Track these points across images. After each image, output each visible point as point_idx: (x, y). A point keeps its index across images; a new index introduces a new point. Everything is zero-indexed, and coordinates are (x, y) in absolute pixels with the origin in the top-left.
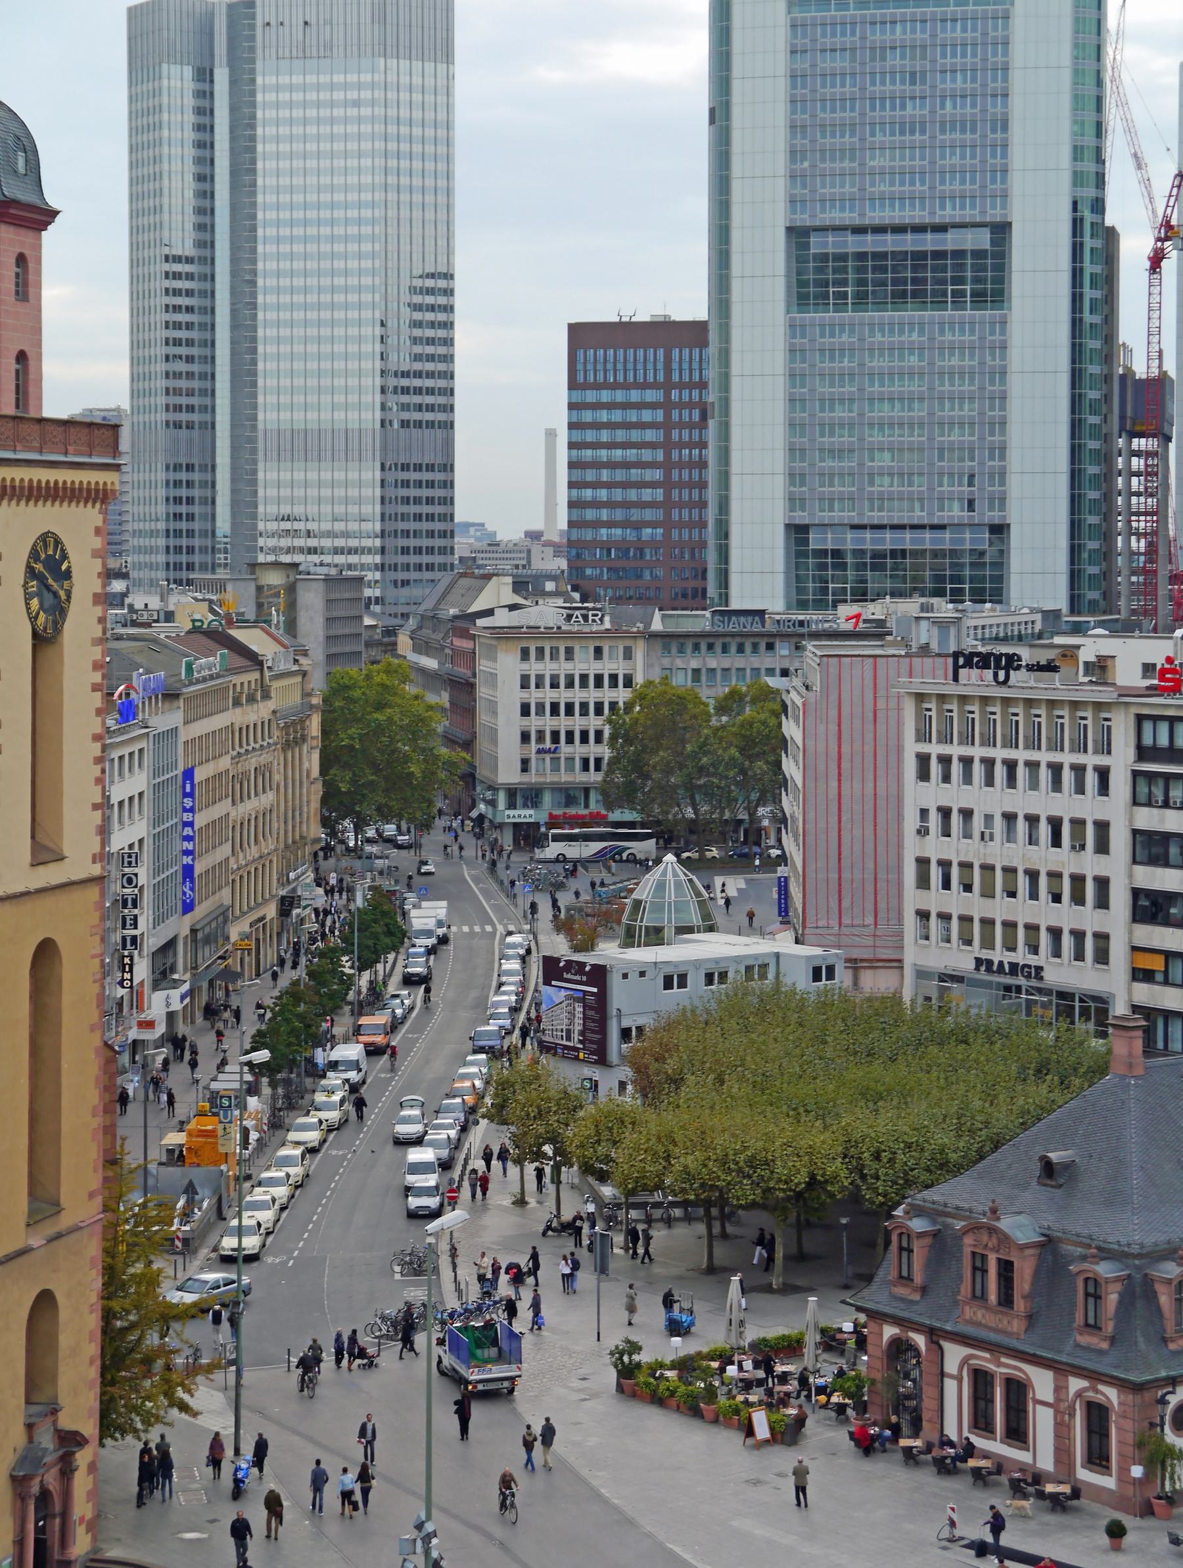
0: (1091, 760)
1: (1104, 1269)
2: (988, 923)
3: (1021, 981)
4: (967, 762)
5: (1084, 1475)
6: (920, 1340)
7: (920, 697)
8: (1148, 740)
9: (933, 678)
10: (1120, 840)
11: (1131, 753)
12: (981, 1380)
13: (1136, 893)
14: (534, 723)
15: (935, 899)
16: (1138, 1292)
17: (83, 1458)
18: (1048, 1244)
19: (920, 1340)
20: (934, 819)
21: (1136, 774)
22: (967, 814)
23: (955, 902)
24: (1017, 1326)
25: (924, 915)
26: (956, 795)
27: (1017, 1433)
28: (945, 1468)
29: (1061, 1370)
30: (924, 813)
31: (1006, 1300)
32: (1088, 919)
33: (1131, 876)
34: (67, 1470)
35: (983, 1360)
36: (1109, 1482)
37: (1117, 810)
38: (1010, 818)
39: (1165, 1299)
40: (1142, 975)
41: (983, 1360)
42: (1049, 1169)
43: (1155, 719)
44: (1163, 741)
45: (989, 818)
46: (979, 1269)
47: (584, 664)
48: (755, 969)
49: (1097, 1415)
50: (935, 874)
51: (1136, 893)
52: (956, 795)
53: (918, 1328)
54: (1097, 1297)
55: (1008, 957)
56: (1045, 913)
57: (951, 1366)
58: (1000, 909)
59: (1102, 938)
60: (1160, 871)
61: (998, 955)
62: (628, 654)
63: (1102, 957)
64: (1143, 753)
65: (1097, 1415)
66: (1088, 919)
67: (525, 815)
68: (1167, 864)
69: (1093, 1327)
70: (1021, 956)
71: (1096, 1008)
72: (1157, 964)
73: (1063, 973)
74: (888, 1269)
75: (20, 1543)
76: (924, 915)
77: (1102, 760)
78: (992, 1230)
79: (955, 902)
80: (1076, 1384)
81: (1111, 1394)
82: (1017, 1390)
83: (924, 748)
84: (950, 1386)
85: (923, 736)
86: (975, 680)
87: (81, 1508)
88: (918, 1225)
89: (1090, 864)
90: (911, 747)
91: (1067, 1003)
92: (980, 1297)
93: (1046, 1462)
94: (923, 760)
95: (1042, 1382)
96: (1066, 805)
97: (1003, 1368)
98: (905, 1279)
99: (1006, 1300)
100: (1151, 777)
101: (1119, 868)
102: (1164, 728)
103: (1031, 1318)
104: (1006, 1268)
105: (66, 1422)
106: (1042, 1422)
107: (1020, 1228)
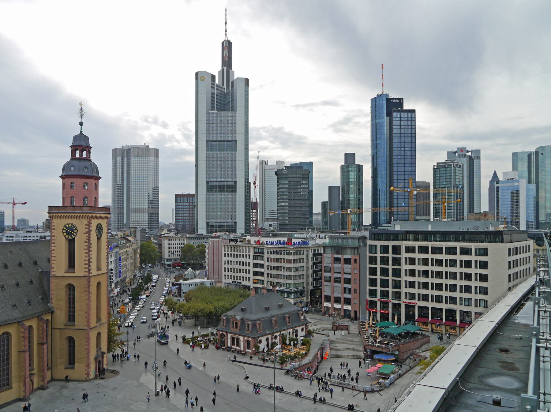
0: (248, 254)
1: (250, 323)
2: (234, 276)
4: (231, 254)
5: (247, 350)
6: (225, 333)
7: (225, 246)
9: (226, 243)
10: (252, 264)
12: (233, 339)
14: (170, 250)
15: (227, 273)
16: (254, 325)
17: (105, 355)
18: (242, 320)
19: (225, 333)
22: (231, 261)
23: (229, 273)
24: (238, 331)
25: (225, 275)
26: (229, 259)
27: (238, 345)
28: (228, 350)
29: (244, 336)
31: (236, 327)
32: (247, 275)
34: (103, 357)
35: (233, 336)
36: (250, 351)
37: (251, 260)
38: (237, 262)
39: (258, 326)
40: (254, 283)
41: (233, 336)
42: (242, 309)
46: (233, 323)
47: (178, 241)
48: (202, 283)
49: (249, 342)
50: (227, 270)
52: (229, 259)
56: (242, 275)
57: (229, 337)
59: (249, 278)
61: (235, 281)
63: (249, 280)
64: (255, 253)
65: (249, 342)
66: (247, 275)
67: (169, 263)
69: (248, 330)
70: (238, 281)
71: (248, 287)
72: (257, 281)
73: (244, 283)
74: (220, 324)
75: (96, 368)
76: (225, 275)
79: (229, 273)
80: (246, 338)
81: (251, 339)
82: (238, 340)
84: (229, 339)
85: (225, 251)
86: (232, 243)
87: (105, 362)
88: (224, 318)
89: (248, 268)
90: (223, 252)
92: (233, 327)
94: (225, 254)
95: (241, 338)
96: (244, 260)
97: (236, 336)
98: (223, 325)
99: (236, 327)
101: (251, 268)
103: (240, 330)
104: (236, 323)
105: (103, 350)
106: (241, 344)
107: (238, 317)
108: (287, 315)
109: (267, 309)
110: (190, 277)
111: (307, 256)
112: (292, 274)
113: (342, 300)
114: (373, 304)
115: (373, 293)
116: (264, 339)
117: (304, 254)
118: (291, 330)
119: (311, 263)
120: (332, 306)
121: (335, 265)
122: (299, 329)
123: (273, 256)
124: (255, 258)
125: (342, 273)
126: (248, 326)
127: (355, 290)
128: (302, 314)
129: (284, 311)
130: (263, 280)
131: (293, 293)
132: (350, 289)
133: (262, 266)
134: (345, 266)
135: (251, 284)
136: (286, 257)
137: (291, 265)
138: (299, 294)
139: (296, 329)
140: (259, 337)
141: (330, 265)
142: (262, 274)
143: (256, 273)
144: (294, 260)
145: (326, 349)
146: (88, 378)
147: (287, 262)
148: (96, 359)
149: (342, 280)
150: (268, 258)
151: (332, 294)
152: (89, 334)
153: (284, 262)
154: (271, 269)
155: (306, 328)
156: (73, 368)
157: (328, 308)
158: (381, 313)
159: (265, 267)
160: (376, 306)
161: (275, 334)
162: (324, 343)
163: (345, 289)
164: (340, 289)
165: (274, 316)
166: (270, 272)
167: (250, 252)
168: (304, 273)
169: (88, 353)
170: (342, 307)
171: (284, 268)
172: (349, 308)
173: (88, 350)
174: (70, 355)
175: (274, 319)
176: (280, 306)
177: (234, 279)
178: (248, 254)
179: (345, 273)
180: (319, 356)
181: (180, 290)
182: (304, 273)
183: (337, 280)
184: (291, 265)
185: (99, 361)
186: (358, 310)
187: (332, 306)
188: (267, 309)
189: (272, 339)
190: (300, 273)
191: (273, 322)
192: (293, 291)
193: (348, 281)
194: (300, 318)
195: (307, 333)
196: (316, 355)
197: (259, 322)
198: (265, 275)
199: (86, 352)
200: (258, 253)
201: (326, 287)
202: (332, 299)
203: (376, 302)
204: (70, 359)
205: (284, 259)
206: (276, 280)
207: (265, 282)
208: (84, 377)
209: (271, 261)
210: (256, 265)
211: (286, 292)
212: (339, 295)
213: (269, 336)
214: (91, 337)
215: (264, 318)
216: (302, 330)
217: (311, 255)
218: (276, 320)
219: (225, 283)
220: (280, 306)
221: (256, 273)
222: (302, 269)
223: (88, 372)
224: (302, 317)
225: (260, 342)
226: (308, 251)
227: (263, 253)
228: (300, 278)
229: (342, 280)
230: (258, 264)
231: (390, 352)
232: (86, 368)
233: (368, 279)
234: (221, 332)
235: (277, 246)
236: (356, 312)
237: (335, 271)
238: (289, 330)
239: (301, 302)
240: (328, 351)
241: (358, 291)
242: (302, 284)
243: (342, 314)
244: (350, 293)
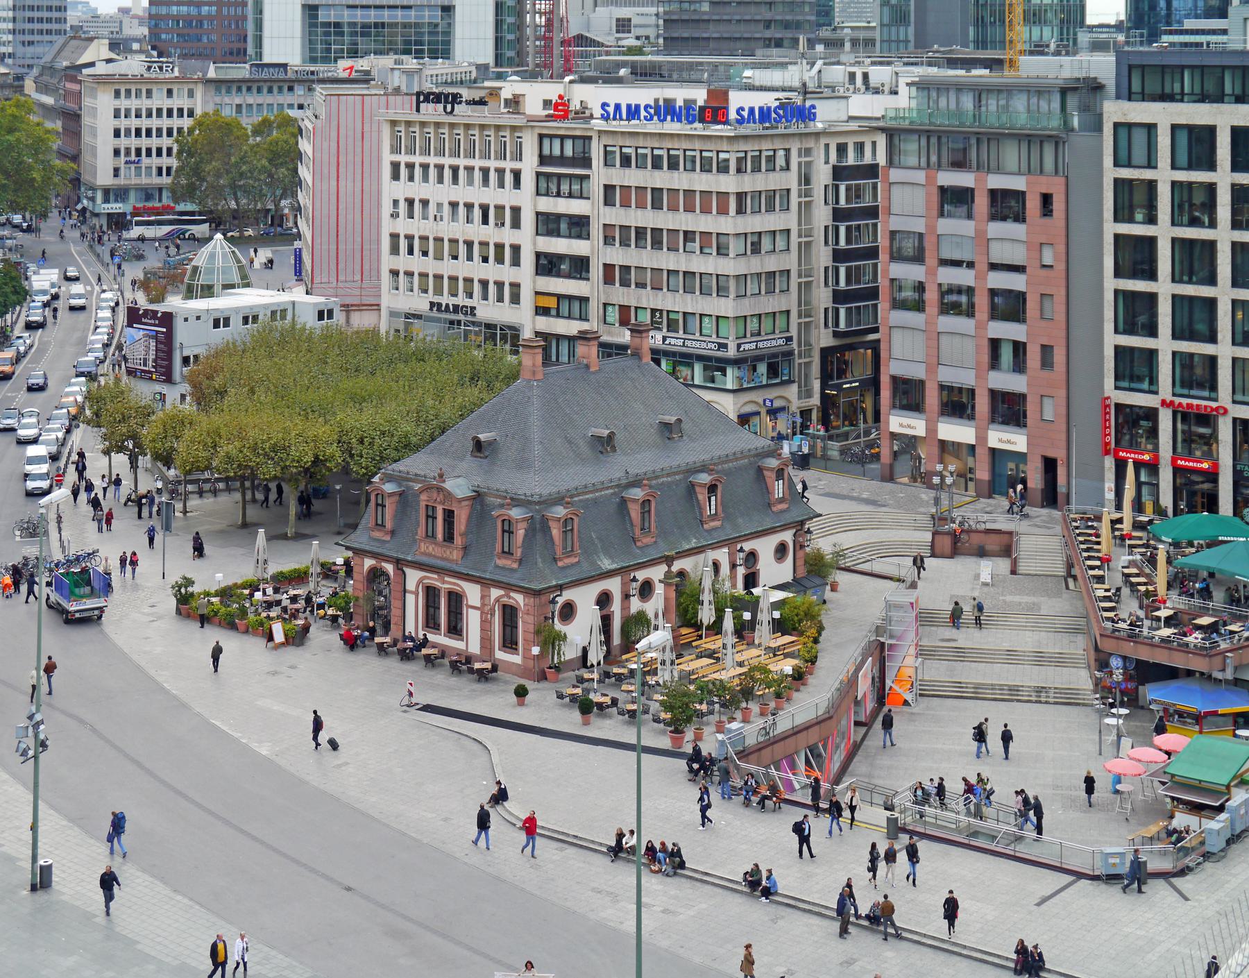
0: (508, 165)
1: (516, 513)
2: (438, 278)
3: (461, 317)
4: (425, 167)
6: (389, 568)
8: (546, 152)
10: (528, 219)
11: (536, 160)
12: (431, 594)
13: (538, 255)
15: (403, 262)
18: (478, 497)
19: (389, 568)
20: (403, 206)
21: (538, 174)
22: (425, 203)
23: (417, 263)
24: (456, 555)
25: (395, 273)
26: (418, 190)
29: (485, 583)
30: (396, 202)
31: (449, 537)
32: (506, 273)
33: (535, 244)
35: (433, 579)
36: (516, 659)
37: (527, 200)
38: (454, 205)
39: (556, 532)
40: (542, 311)
43: (551, 137)
44: (557, 152)
45: (440, 205)
46: (431, 517)
47: (159, 100)
48: (278, 313)
49: (510, 613)
50: (403, 244)
51: (538, 255)
52: (418, 190)
53: (388, 559)
54: (510, 533)
55: (453, 301)
56: (477, 270)
57: (411, 584)
58: (447, 267)
59: (515, 286)
60: (554, 240)
61: (446, 299)
62: (191, 94)
63: (515, 299)
64: (543, 160)
65: (510, 613)
66: (506, 273)
68: (559, 235)
70: (461, 300)
71: (510, 335)
72: (552, 303)
73: (490, 311)
74: (368, 519)
76: (395, 273)
79: (417, 263)
80: (495, 593)
81: (519, 599)
82: (456, 600)
84: (410, 599)
88: (389, 488)
89: (507, 236)
91: (491, 331)
92: (431, 536)
93: (474, 647)
95: (472, 593)
96: (492, 196)
97: (446, 584)
99: (449, 537)
100: (548, 176)
101: (528, 239)
102: (557, 143)
104: (449, 515)
106: (472, 621)
107: (459, 487)
108: (705, 478)
109: (605, 444)
110: (217, 280)
111: (806, 179)
112: (729, 266)
113: (982, 404)
114: (1133, 424)
115: (1136, 368)
117: (788, 168)
118: (722, 555)
119: (822, 215)
120: (932, 430)
121: (945, 226)
122: (765, 547)
123: (633, 177)
124: (546, 184)
125: (982, 265)
126: (508, 530)
127: (1046, 350)
128: (780, 474)
129: (688, 453)
130: (584, 300)
131: (736, 362)
132: (1019, 348)
133: (579, 226)
134: (996, 229)
136: (702, 182)
137: (727, 224)
138: (762, 368)
139: (748, 546)
140: (561, 588)
141: (919, 226)
142: (580, 266)
143: (548, 265)
144: (741, 196)
145: (899, 654)
147: (706, 210)
149: (982, 302)
150: (609, 189)
151: (932, 369)
153: (689, 209)
154: (625, 243)
155: (799, 546)
157: (910, 443)
158: (1177, 470)
159: (596, 230)
160: (1153, 433)
161: (641, 575)
162: (887, 619)
163: (995, 344)
164: (969, 346)
165: (636, 483)
166: (618, 256)
168: (791, 261)
170: (982, 438)
171: (689, 236)
172: (1017, 441)
175: (638, 493)
177: (439, 291)
179: (994, 267)
180: (864, 686)
181: (166, 344)
183: (956, 302)
184: (727, 224)
186: (1059, 453)
187: (932, 430)
188: (605, 444)
189: (626, 597)
190: (771, 264)
191: (635, 511)
192: (732, 352)
193: (1010, 306)
194: (768, 491)
195: (802, 572)
196: (852, 682)
197: (560, 511)
198: (596, 271)
200: (562, 160)
201: (897, 336)
202: (932, 398)
203: (1151, 414)
205: (689, 193)
207: (594, 309)
209: (626, 204)
210: (549, 224)
211: (700, 358)
212: (965, 378)
213: (614, 585)
215: (585, 489)
216: (781, 550)
217: (822, 175)
218: (646, 503)
219: (393, 314)
221: (548, 265)
222: (781, 244)
224: (779, 489)
225: (568, 611)
226: (808, 152)
227: (586, 162)
228: (770, 291)
229: (982, 302)
230: (558, 217)
231: (1229, 675)
233: (1109, 297)
234: (369, 563)
235: (654, 127)
236: (1050, 465)
237: (947, 254)
238: (712, 555)
239: (773, 412)
240: (910, 661)
241: (1059, 356)
242: (781, 322)
243: (983, 474)
244: (1019, 366)
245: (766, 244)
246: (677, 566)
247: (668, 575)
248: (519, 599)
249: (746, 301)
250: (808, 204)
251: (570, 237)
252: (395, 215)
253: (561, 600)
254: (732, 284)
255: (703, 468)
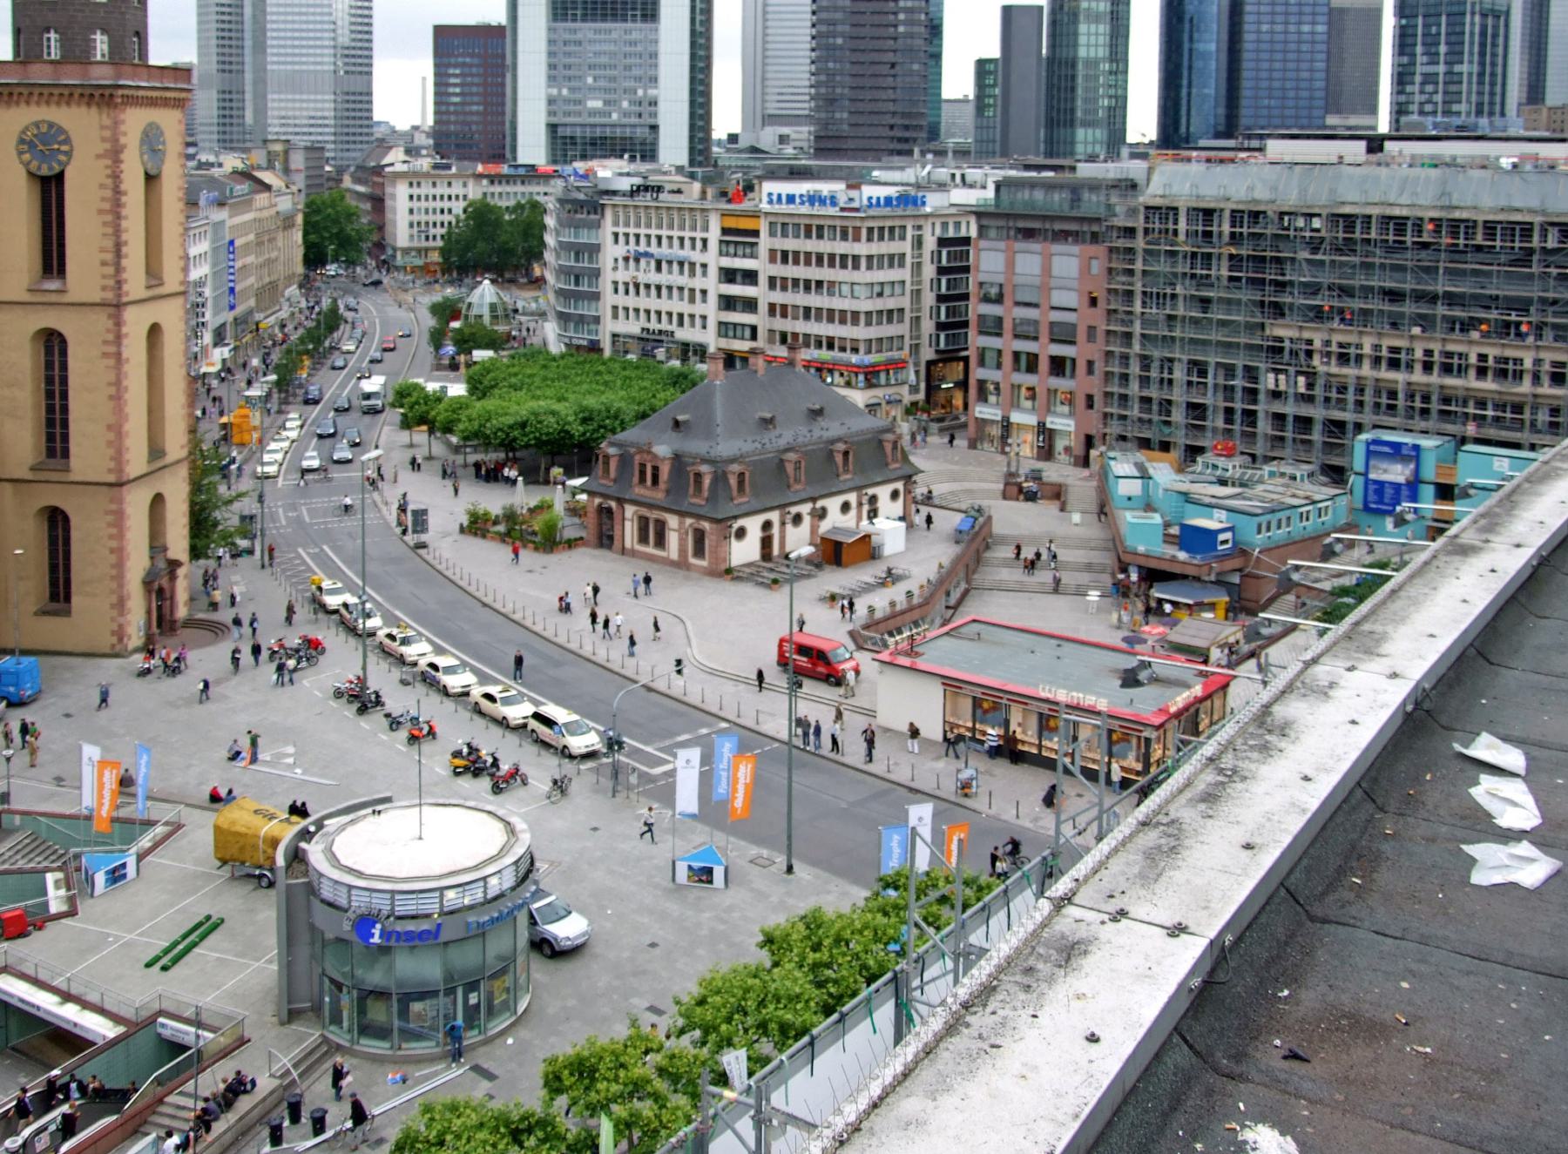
1: (704, 468)
5: (693, 561)
6: (613, 504)
12: (643, 523)
16: (720, 478)
17: (181, 572)
19: (613, 504)
23: (631, 301)
29: (682, 514)
34: (173, 577)
35: (645, 512)
36: (704, 563)
37: (713, 259)
49: (700, 537)
50: (621, 288)
51: (721, 296)
59: (704, 318)
75: (149, 612)
77: (704, 235)
78: (649, 452)
80: (689, 521)
81: (706, 525)
82: (661, 527)
83: (616, 229)
84: (628, 524)
85: (616, 224)
87: (182, 595)
88: (612, 451)
94: (616, 235)
95: (672, 521)
99: (655, 481)
100: (728, 243)
101: (714, 286)
103: (668, 492)
104: (656, 469)
105: (172, 555)
106: (673, 539)
107: (662, 450)
109: (768, 423)
111: (918, 242)
116: (753, 525)
118: (852, 498)
122: (883, 492)
126: (698, 476)
133: (750, 277)
135: (710, 339)
139: (871, 491)
140: (736, 517)
142: (750, 305)
143: (728, 303)
144: (870, 258)
146: (118, 648)
148: (147, 583)
150: (772, 252)
152: (120, 501)
154: (784, 288)
155: (908, 491)
156: (68, 613)
159: (763, 280)
161: (794, 510)
166: (778, 297)
167: (706, 229)
168: (905, 302)
169: (120, 565)
173: (119, 553)
174: (53, 568)
175: (792, 456)
176: (817, 413)
178: (699, 235)
182: (905, 302)
185: (159, 590)
189: (783, 524)
190: (891, 303)
191: (790, 468)
197: (736, 468)
199: (113, 559)
204: (54, 583)
206: (801, 327)
207: (761, 333)
208: (106, 641)
210: (729, 275)
213: (774, 516)
214: (129, 510)
216: (895, 495)
217: (930, 243)
220: (817, 413)
221: (728, 303)
222: (898, 289)
223: (121, 626)
225: (741, 533)
231: (1213, 578)
232: (114, 613)
234: (597, 501)
237: (1019, 298)
245: (887, 291)
246: (819, 504)
247: (814, 509)
248: (706, 525)
249: (871, 329)
250: (919, 264)
251: (744, 283)
252: (615, 269)
253: (736, 526)
254: (862, 318)
255: (839, 440)
